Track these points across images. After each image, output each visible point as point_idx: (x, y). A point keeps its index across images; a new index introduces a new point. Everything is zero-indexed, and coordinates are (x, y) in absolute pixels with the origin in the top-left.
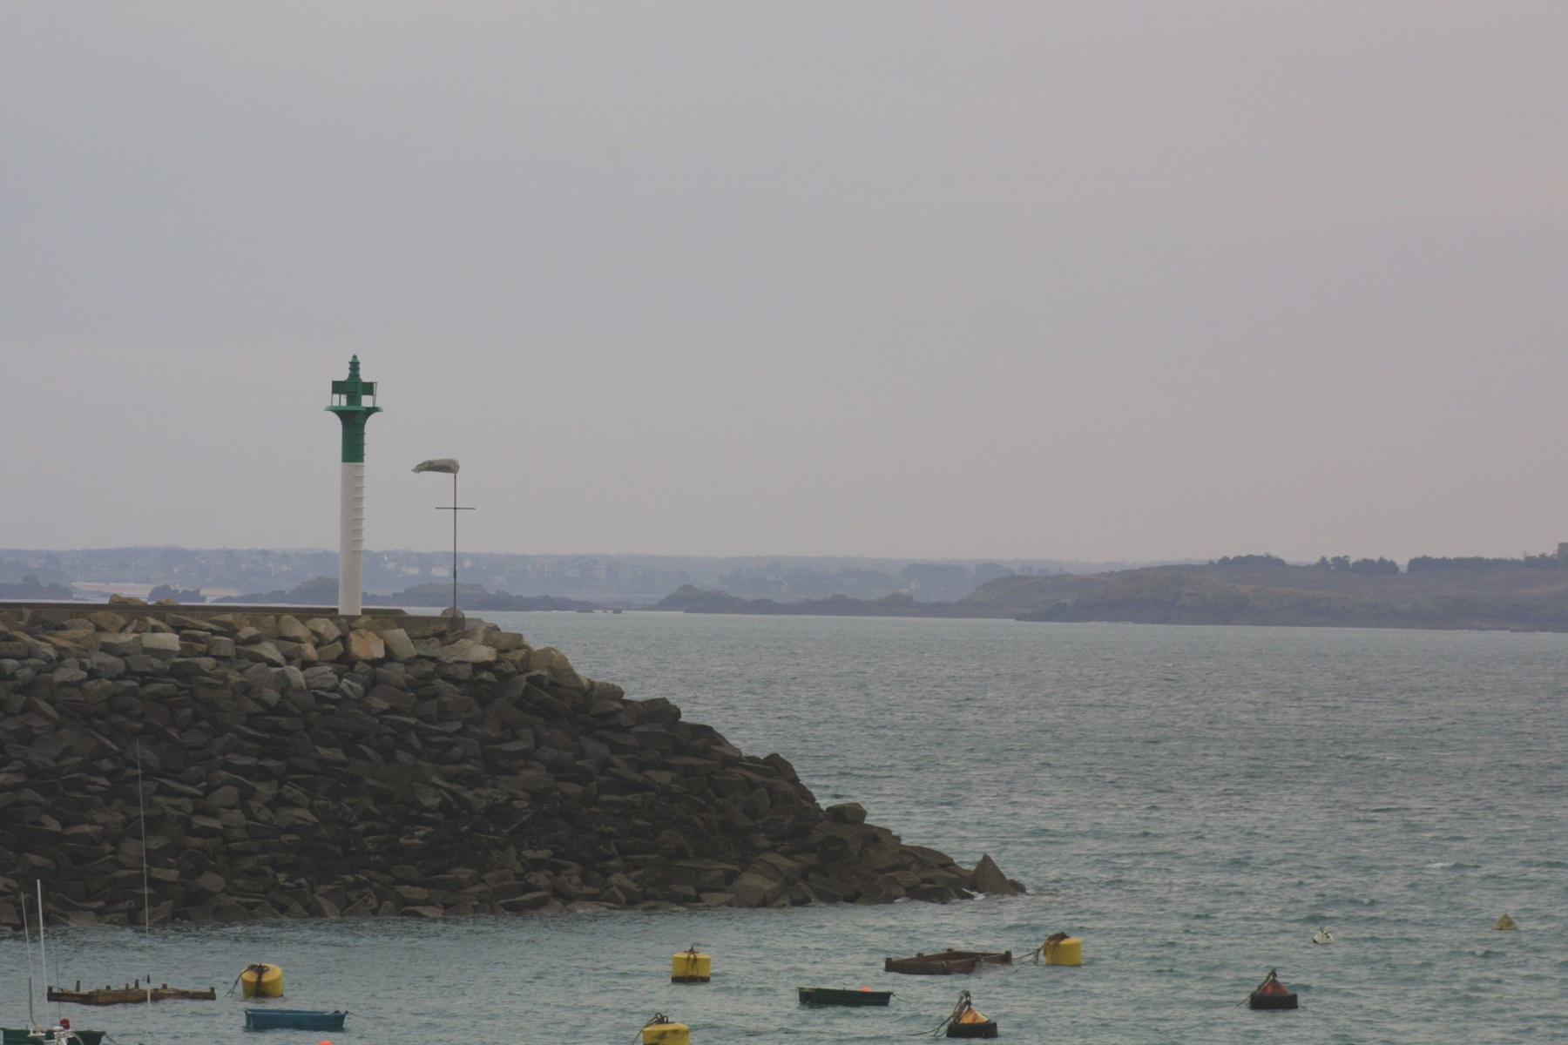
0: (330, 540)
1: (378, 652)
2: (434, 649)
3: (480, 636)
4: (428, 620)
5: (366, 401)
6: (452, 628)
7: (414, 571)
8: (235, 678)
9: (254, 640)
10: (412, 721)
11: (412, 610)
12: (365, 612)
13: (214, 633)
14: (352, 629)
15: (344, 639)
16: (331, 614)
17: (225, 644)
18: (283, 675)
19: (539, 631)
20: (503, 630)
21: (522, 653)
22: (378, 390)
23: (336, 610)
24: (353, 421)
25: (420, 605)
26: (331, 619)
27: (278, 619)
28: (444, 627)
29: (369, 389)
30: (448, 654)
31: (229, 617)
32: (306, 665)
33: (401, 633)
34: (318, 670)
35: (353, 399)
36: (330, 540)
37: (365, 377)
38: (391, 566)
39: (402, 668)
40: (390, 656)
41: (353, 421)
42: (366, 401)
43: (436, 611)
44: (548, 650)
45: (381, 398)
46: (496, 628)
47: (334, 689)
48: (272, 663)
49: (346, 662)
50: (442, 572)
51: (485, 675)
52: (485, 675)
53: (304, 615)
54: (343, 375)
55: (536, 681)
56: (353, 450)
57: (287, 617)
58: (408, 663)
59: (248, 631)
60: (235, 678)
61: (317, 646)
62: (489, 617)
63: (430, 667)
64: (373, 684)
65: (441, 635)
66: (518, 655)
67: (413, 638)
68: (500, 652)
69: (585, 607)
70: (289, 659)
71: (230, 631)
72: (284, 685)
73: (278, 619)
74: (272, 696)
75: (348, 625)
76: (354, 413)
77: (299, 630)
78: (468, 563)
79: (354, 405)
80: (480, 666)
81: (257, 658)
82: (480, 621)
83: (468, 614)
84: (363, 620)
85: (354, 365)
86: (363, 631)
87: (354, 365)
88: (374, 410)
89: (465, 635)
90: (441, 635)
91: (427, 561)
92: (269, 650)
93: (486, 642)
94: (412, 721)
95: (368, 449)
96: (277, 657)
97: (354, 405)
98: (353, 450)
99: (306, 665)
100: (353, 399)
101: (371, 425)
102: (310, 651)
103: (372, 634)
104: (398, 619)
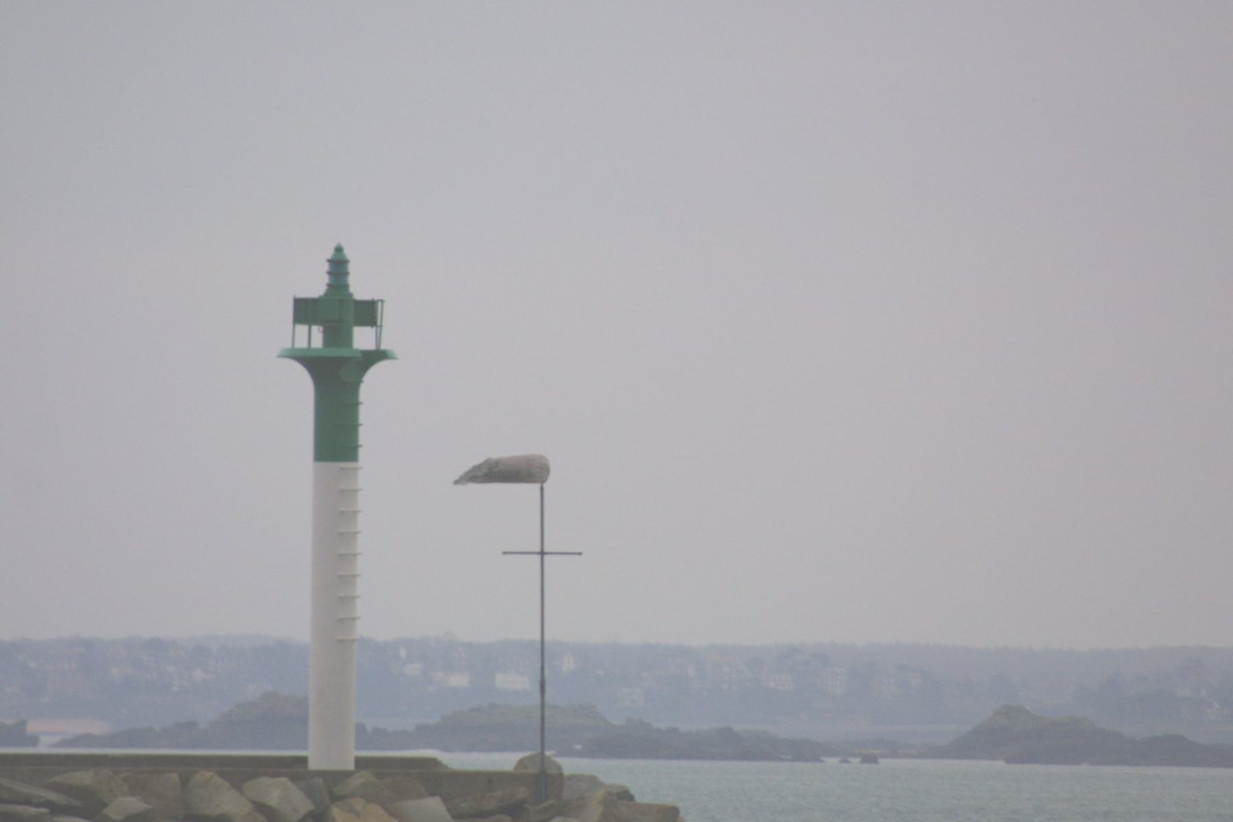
0: (290, 617)
4: (490, 779)
5: (363, 339)
7: (459, 680)
11: (457, 760)
12: (361, 763)
13: (56, 810)
14: (335, 798)
16: (294, 768)
20: (639, 799)
22: (387, 315)
23: (303, 760)
24: (336, 380)
25: (470, 748)
26: (294, 778)
27: (185, 781)
28: (522, 793)
29: (368, 313)
31: (85, 778)
35: (337, 333)
37: (360, 289)
38: (413, 669)
41: (336, 380)
42: (363, 339)
43: (506, 761)
45: (393, 331)
46: (625, 795)
50: (516, 683)
53: (240, 771)
54: (316, 286)
56: (336, 437)
57: (204, 775)
62: (614, 772)
69: (804, 751)
73: (185, 781)
76: (340, 362)
78: (568, 664)
79: (337, 343)
82: (593, 781)
83: (570, 765)
84: (357, 781)
85: (338, 266)
86: (358, 804)
87: (338, 266)
88: (377, 355)
97: (337, 343)
98: (336, 437)
100: (337, 333)
101: (374, 388)
103: (374, 808)
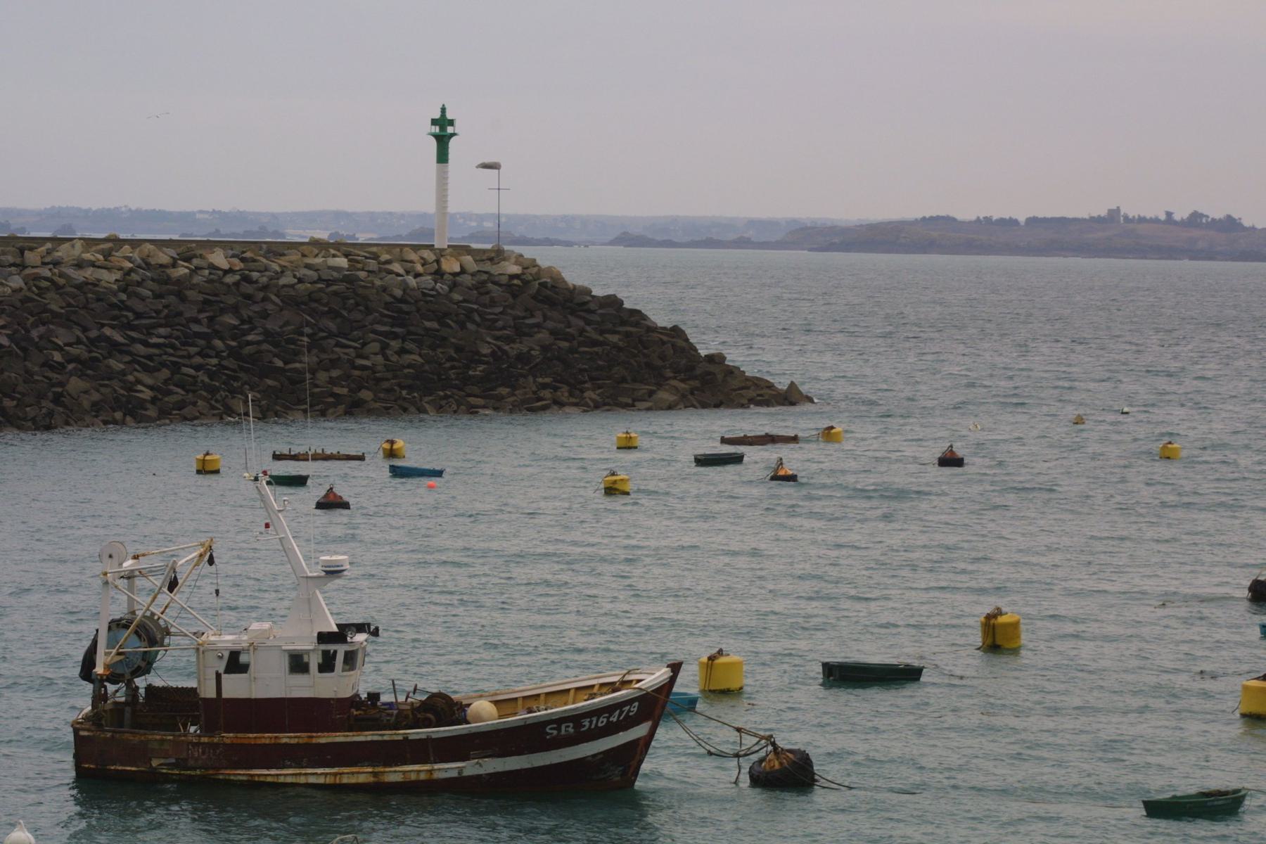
0: (427, 204)
1: (457, 269)
2: (487, 267)
3: (513, 260)
4: (484, 251)
5: (450, 130)
6: (497, 255)
7: (474, 224)
8: (378, 283)
9: (388, 262)
10: (475, 307)
11: (475, 246)
15: (438, 261)
16: (431, 247)
17: (373, 264)
18: (404, 281)
19: (545, 258)
21: (536, 269)
22: (457, 123)
24: (443, 141)
29: (451, 123)
30: (495, 270)
31: (374, 249)
32: (417, 275)
33: (469, 258)
34: (423, 278)
35: (443, 128)
36: (427, 204)
37: (449, 116)
38: (461, 221)
39: (470, 277)
40: (463, 271)
41: (443, 141)
42: (450, 130)
43: (489, 246)
44: (550, 268)
45: (458, 128)
46: (521, 256)
47: (432, 289)
48: (398, 275)
49: (439, 274)
50: (489, 225)
51: (516, 282)
52: (516, 282)
53: (416, 248)
54: (437, 115)
55: (543, 285)
56: (443, 157)
58: (473, 275)
59: (384, 257)
60: (378, 283)
61: (423, 265)
62: (518, 249)
63: (485, 277)
64: (454, 286)
65: (491, 259)
66: (535, 270)
67: (476, 261)
68: (525, 268)
69: (568, 244)
70: (408, 272)
71: (375, 257)
72: (405, 287)
74: (398, 293)
75: (440, 253)
77: (413, 256)
80: (513, 277)
81: (390, 272)
83: (506, 248)
85: (443, 110)
87: (443, 110)
89: (504, 260)
90: (491, 259)
91: (481, 218)
92: (397, 267)
93: (516, 263)
94: (475, 307)
95: (450, 156)
96: (401, 271)
98: (443, 157)
99: (417, 275)
100: (443, 128)
101: (453, 143)
102: (419, 268)
104: (468, 250)
